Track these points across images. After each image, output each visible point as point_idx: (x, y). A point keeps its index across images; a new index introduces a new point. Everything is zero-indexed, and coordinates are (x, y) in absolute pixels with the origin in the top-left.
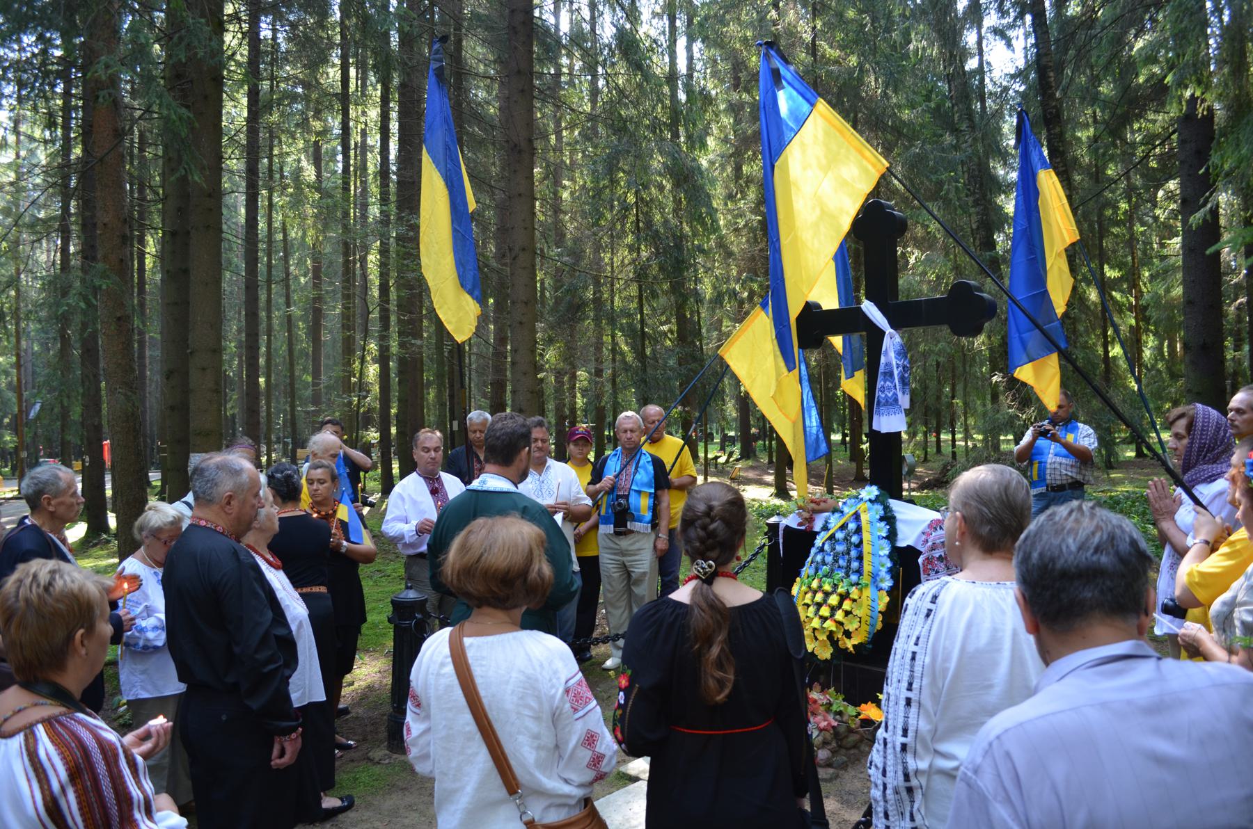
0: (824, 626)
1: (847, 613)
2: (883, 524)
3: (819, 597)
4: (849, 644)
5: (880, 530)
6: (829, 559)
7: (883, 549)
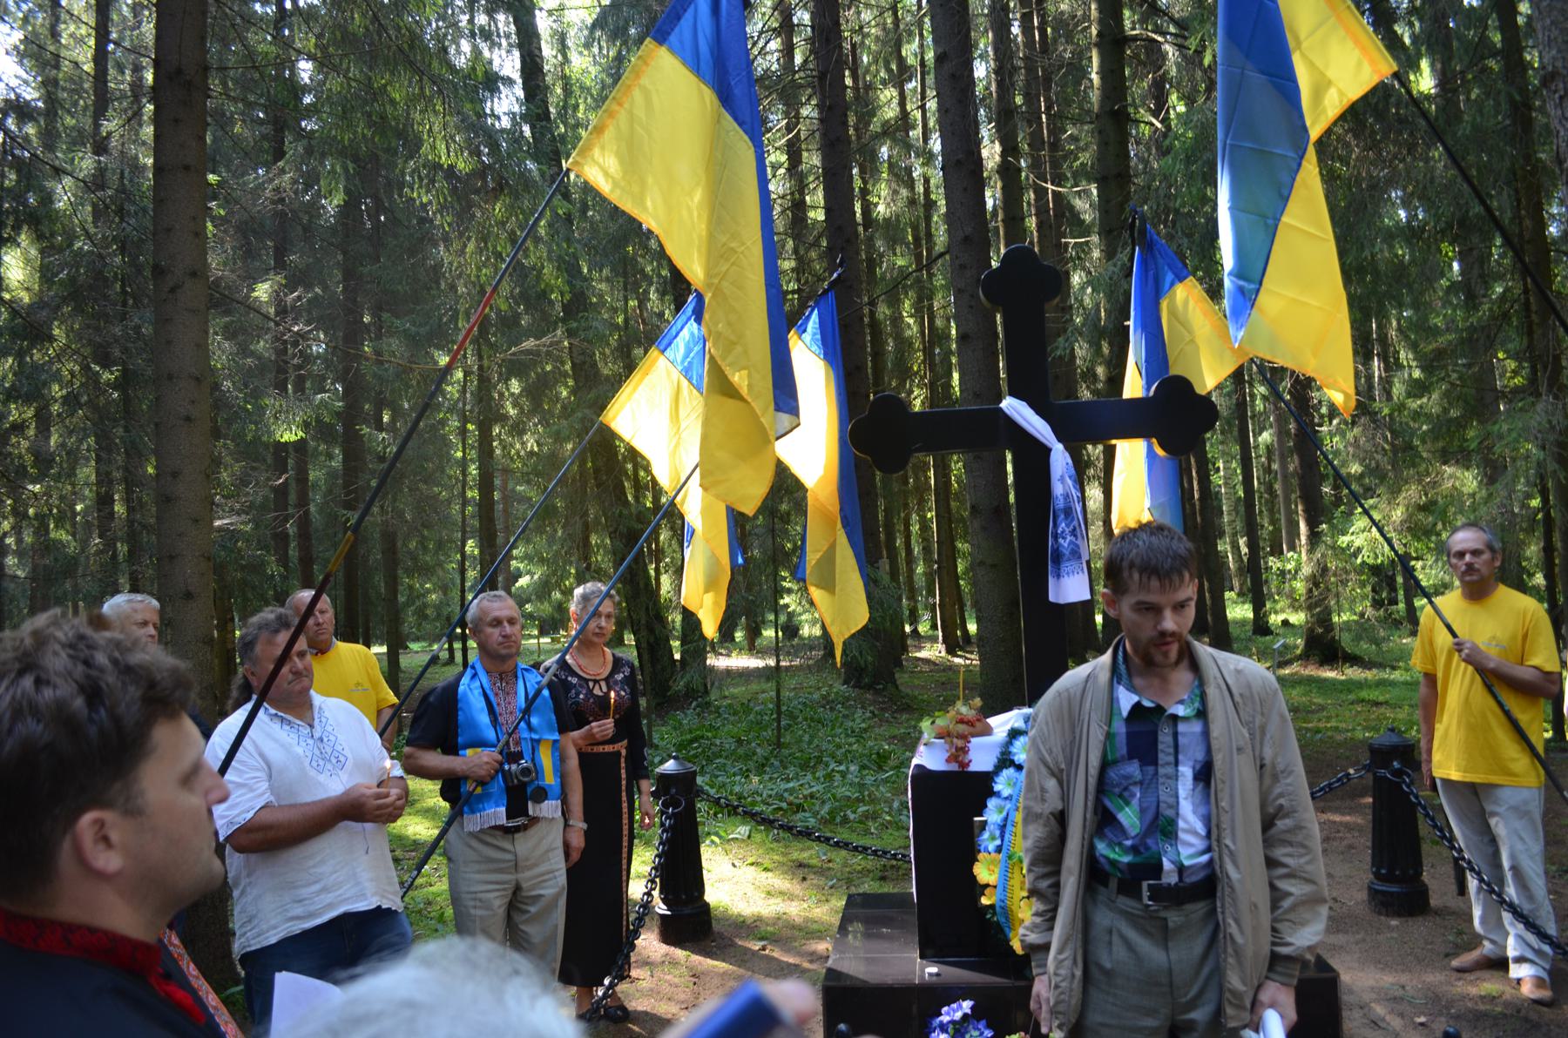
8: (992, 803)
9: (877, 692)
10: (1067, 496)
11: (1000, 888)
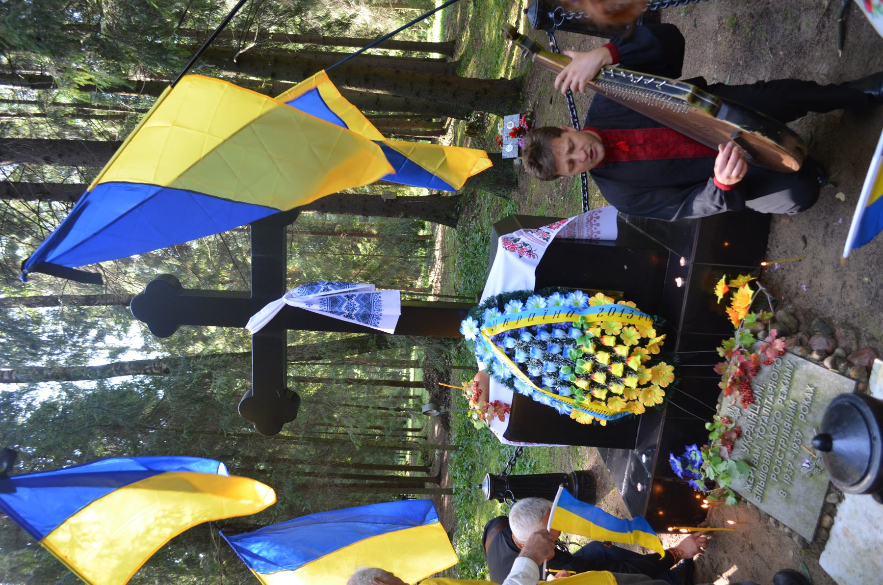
0: (635, 369)
1: (619, 341)
2: (508, 308)
3: (600, 378)
4: (656, 340)
5: (514, 308)
6: (551, 367)
7: (537, 306)
8: (537, 398)
9: (462, 210)
10: (322, 301)
11: (596, 416)
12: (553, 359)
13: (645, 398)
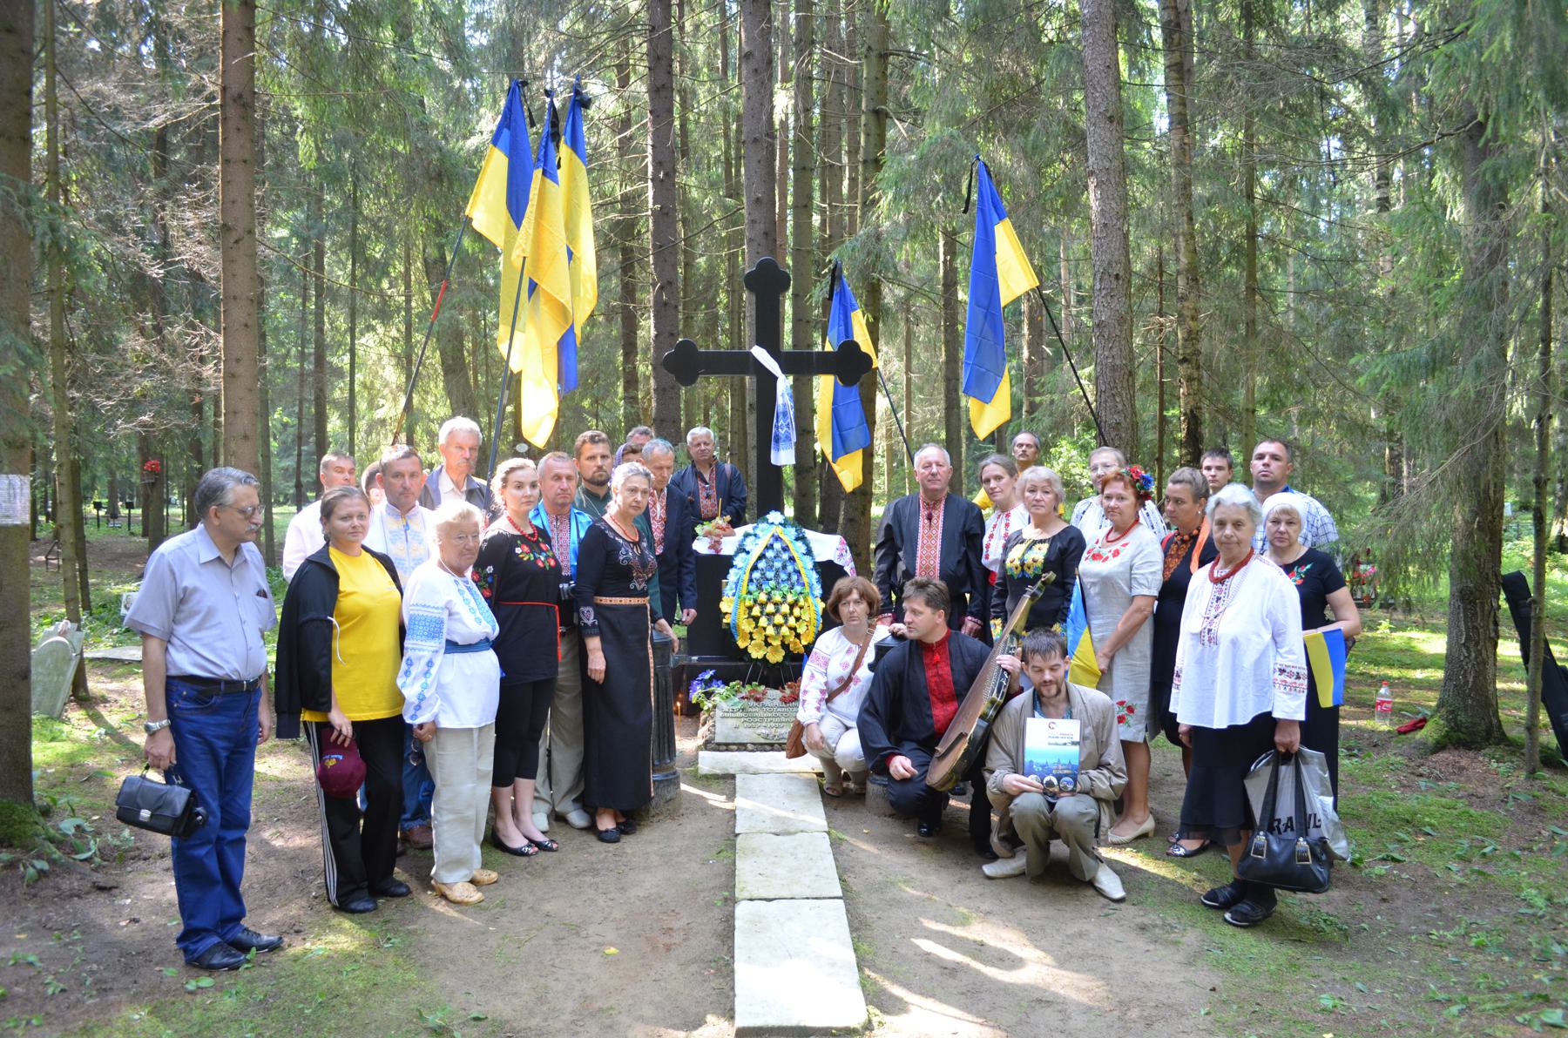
1: (798, 619)
2: (799, 544)
6: (770, 574)
8: (732, 571)
10: (784, 405)
12: (777, 576)
13: (755, 645)
